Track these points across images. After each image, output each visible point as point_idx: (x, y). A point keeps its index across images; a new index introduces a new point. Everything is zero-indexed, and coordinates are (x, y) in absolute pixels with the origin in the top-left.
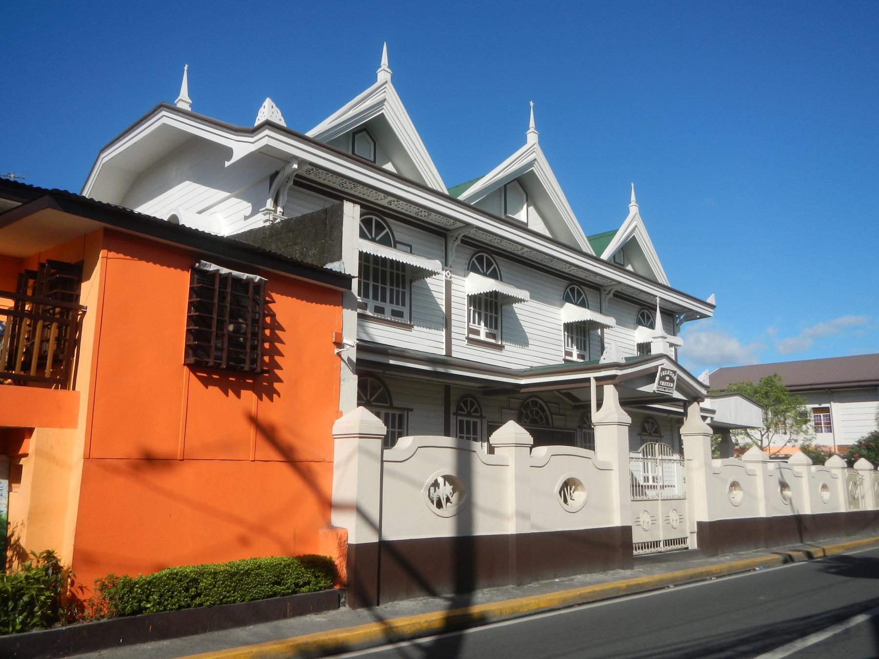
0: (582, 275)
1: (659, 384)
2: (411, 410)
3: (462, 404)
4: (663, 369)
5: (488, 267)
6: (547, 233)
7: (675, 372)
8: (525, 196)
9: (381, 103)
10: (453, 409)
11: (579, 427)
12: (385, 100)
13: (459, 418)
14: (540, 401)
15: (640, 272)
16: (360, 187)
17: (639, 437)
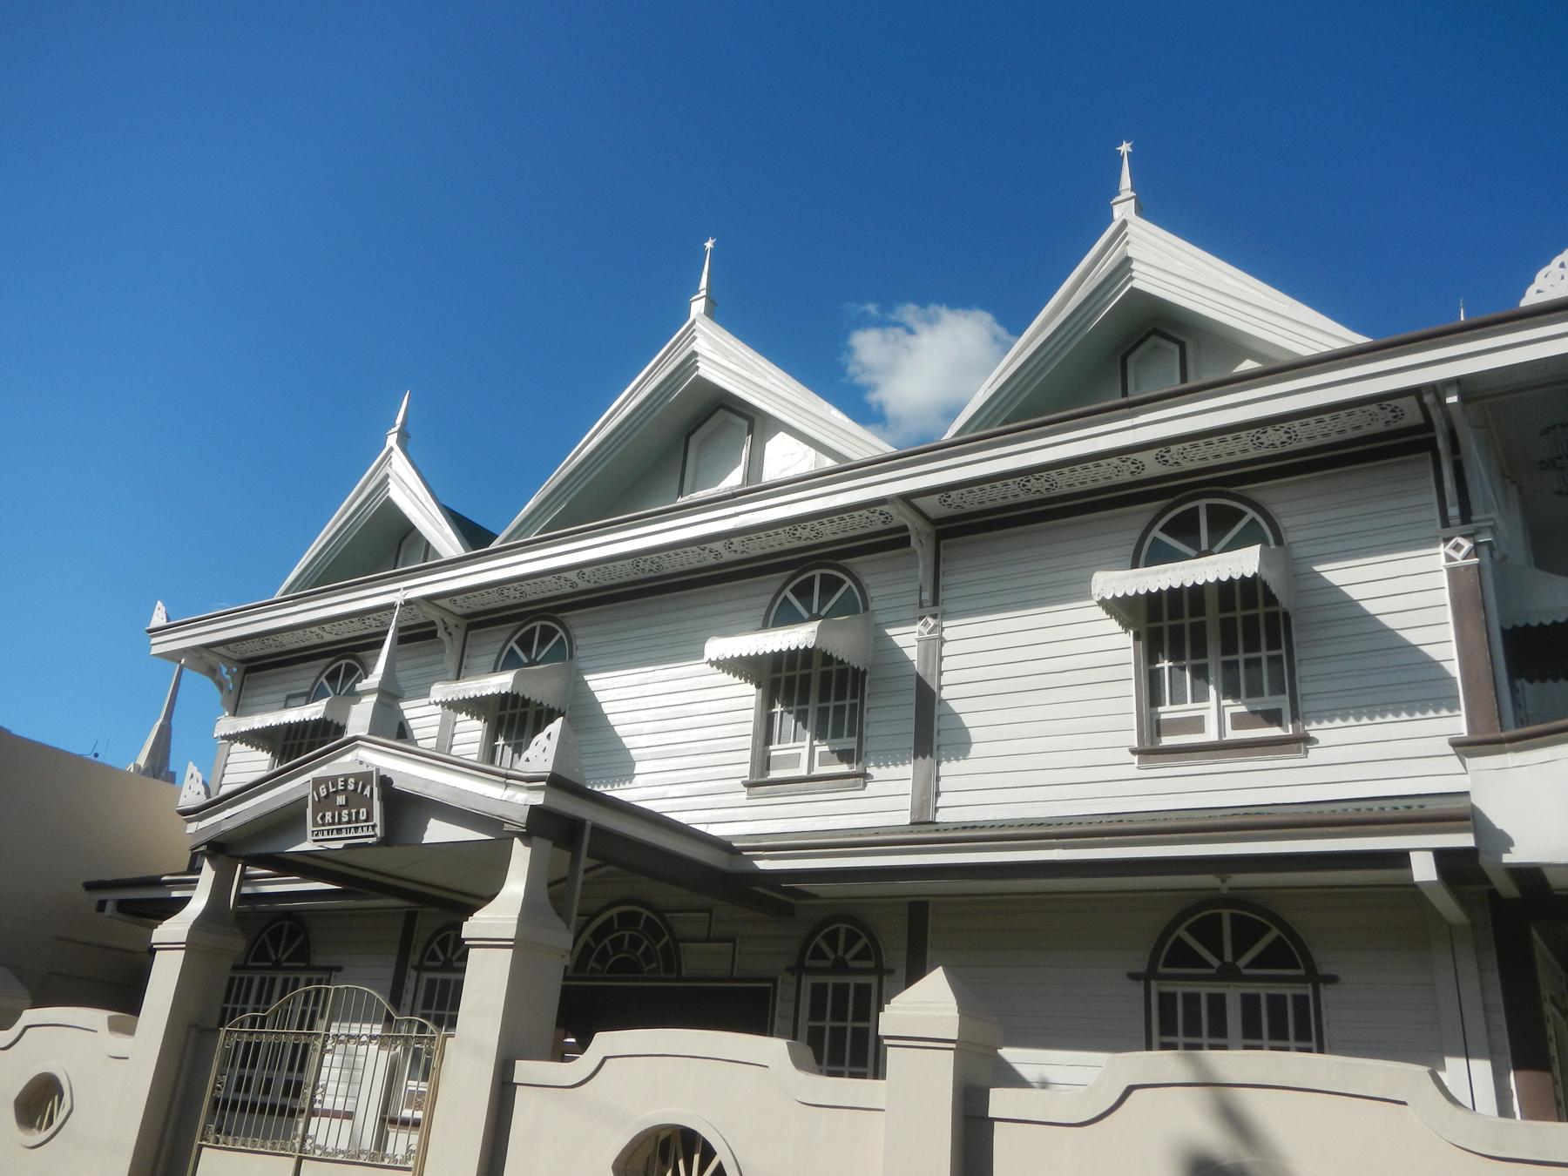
0: (806, 536)
1: (315, 824)
2: (339, 969)
3: (435, 945)
4: (317, 782)
5: (544, 641)
6: (829, 463)
7: (365, 778)
8: (745, 424)
9: (384, 482)
10: (415, 958)
11: (790, 969)
12: (387, 476)
13: (427, 976)
14: (646, 913)
15: (1285, 360)
16: (280, 637)
17: (1139, 988)
